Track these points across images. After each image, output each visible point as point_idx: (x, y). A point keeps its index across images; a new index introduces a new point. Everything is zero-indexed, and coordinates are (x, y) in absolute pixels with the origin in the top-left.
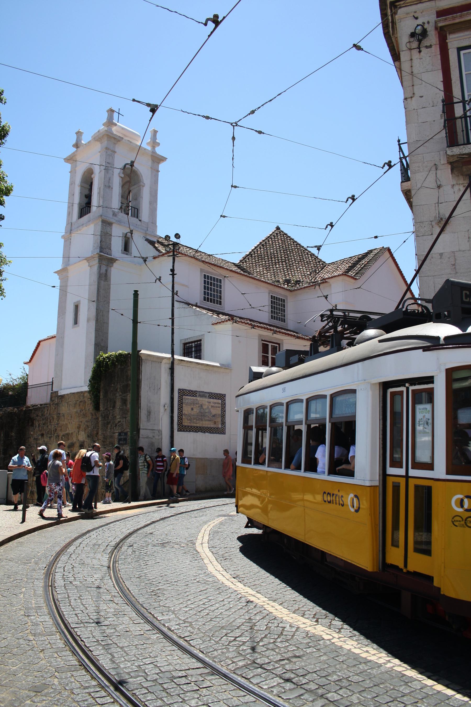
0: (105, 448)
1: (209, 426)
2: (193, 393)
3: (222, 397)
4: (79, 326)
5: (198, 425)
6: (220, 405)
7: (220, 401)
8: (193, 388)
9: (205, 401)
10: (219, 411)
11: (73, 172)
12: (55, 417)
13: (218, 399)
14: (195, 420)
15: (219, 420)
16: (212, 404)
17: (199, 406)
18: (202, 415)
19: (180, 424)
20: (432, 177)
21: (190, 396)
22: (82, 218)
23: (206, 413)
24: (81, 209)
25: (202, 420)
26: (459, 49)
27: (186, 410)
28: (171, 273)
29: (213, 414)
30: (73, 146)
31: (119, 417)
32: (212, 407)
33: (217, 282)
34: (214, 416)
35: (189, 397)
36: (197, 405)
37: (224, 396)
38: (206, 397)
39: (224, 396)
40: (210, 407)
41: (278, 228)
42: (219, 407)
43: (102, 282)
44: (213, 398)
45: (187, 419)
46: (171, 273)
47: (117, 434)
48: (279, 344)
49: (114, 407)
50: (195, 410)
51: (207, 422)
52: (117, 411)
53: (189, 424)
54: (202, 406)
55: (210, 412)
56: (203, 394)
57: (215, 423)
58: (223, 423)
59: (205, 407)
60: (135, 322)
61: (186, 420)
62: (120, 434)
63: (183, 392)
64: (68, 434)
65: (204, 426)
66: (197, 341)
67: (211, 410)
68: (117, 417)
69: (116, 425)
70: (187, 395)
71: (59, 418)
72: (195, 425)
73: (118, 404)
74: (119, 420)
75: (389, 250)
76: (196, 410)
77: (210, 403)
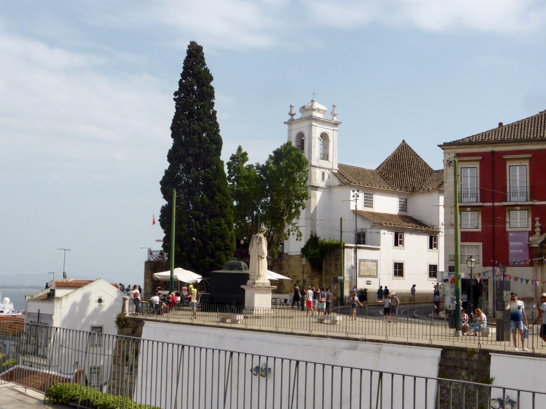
3: (376, 261)
8: (364, 258)
10: (375, 268)
11: (290, 131)
12: (287, 266)
15: (375, 272)
18: (368, 270)
19: (359, 274)
20: (450, 210)
26: (461, 168)
27: (362, 268)
30: (289, 114)
41: (404, 141)
47: (332, 279)
54: (368, 266)
58: (377, 273)
60: (341, 232)
62: (334, 279)
63: (360, 260)
64: (296, 276)
71: (289, 267)
73: (333, 266)
76: (366, 268)
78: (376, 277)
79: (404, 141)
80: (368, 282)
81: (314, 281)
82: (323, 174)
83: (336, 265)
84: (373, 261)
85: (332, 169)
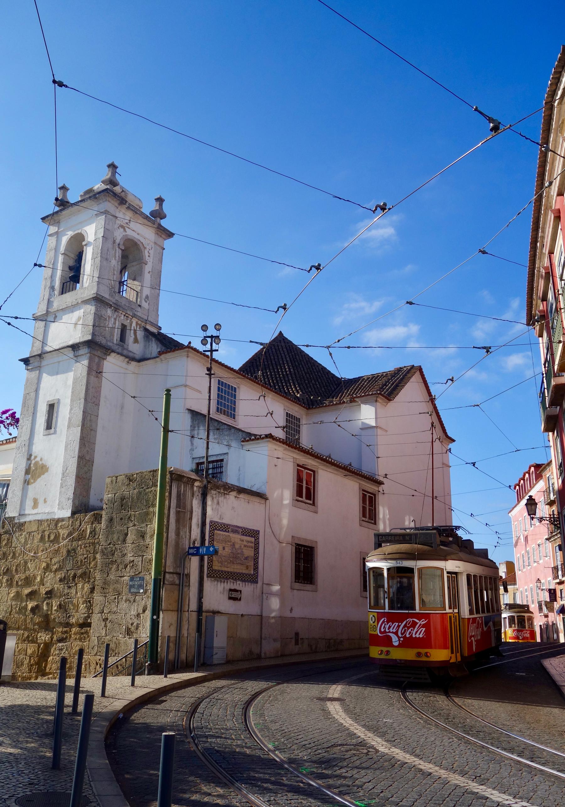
0: (105, 596)
1: (241, 571)
2: (226, 528)
3: (254, 534)
4: (55, 433)
5: (229, 570)
6: (253, 545)
7: (253, 539)
8: (226, 521)
9: (236, 538)
10: (249, 552)
13: (252, 537)
14: (226, 563)
15: (251, 563)
16: (245, 543)
17: (231, 545)
18: (235, 557)
19: (210, 567)
21: (222, 530)
22: (64, 295)
23: (238, 553)
24: (64, 284)
25: (233, 563)
28: (208, 372)
29: (246, 556)
31: (131, 555)
32: (245, 546)
33: (232, 390)
34: (246, 558)
35: (221, 533)
36: (229, 543)
37: (257, 532)
38: (238, 533)
39: (257, 532)
40: (243, 546)
42: (252, 547)
43: (92, 378)
44: (246, 535)
45: (218, 561)
46: (208, 372)
48: (314, 472)
49: (124, 541)
50: (227, 549)
51: (239, 567)
52: (129, 546)
53: (220, 569)
54: (234, 545)
55: (242, 553)
56: (236, 529)
57: (247, 568)
58: (256, 568)
59: (237, 546)
60: (166, 430)
61: (217, 562)
62: (132, 579)
63: (215, 526)
65: (235, 571)
66: (217, 461)
67: (244, 550)
68: (129, 555)
69: (126, 567)
70: (219, 530)
72: (226, 569)
73: (131, 537)
74: (132, 559)
75: (420, 369)
76: (228, 550)
77: (243, 541)
78: (253, 579)
79: (281, 332)
80: (234, 595)
81: (73, 591)
82: (124, 329)
83: (142, 535)
84: (247, 532)
85: (146, 321)
